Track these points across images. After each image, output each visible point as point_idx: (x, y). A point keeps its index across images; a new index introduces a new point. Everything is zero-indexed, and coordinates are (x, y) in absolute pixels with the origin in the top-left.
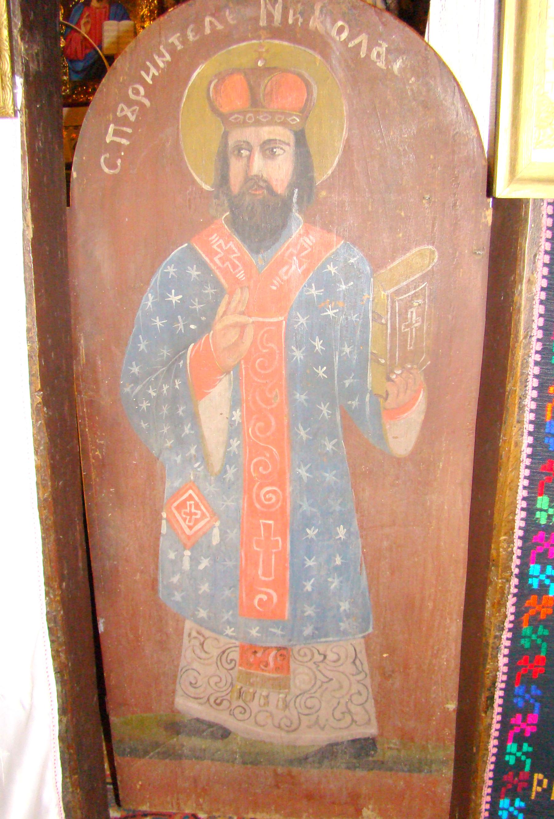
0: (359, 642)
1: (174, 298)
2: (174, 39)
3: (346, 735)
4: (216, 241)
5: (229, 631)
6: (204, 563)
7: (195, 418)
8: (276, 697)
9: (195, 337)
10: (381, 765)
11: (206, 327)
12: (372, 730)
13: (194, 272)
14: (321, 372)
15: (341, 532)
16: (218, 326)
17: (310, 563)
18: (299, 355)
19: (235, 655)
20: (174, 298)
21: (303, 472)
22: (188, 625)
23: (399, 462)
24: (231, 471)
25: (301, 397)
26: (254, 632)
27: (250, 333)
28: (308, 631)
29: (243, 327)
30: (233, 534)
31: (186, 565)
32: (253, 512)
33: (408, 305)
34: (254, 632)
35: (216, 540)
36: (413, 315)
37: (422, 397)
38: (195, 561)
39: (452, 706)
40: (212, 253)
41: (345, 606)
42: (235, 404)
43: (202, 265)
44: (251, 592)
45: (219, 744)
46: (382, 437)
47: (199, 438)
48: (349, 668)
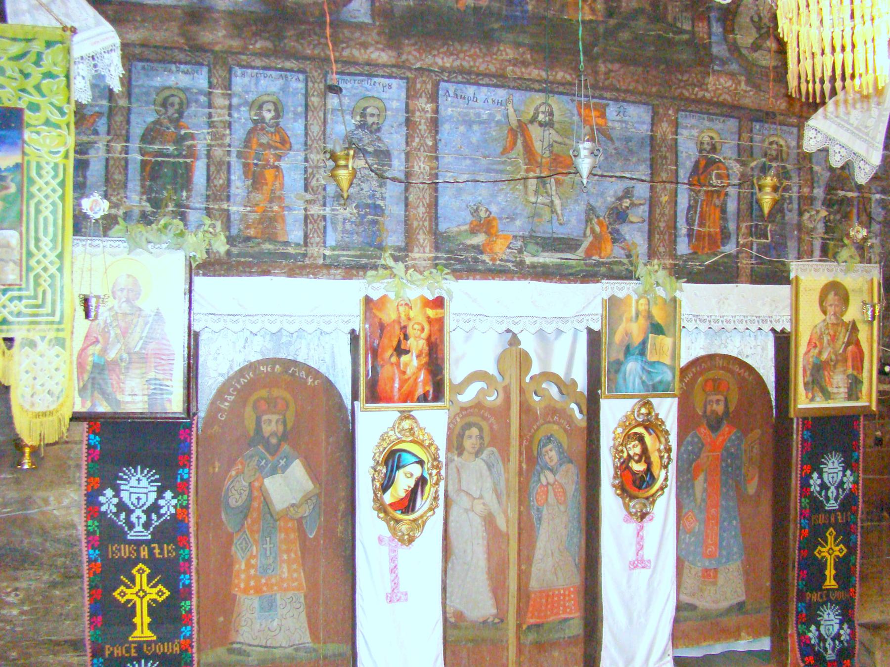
0: (738, 563)
1: (690, 448)
2: (694, 370)
3: (734, 602)
4: (702, 430)
5: (699, 564)
6: (693, 539)
7: (693, 485)
8: (713, 589)
9: (694, 460)
10: (746, 613)
11: (698, 457)
12: (743, 598)
13: (696, 440)
14: (730, 469)
15: (734, 522)
16: (702, 456)
17: (725, 535)
18: (724, 465)
19: (700, 574)
20: (690, 448)
21: (723, 503)
22: (686, 563)
23: (751, 497)
24: (703, 504)
25: (724, 478)
26: (707, 564)
27: (710, 459)
28: (724, 560)
29: (708, 457)
30: (702, 527)
31: (687, 540)
32: (709, 519)
33: (753, 447)
34: (707, 564)
35: (696, 530)
36: (755, 450)
37: (757, 475)
38: (690, 538)
39: (768, 584)
40: (700, 433)
41: (735, 550)
42: (706, 480)
43: (698, 437)
44: (707, 547)
45: (693, 613)
46: (746, 489)
47: (694, 495)
48: (735, 574)
